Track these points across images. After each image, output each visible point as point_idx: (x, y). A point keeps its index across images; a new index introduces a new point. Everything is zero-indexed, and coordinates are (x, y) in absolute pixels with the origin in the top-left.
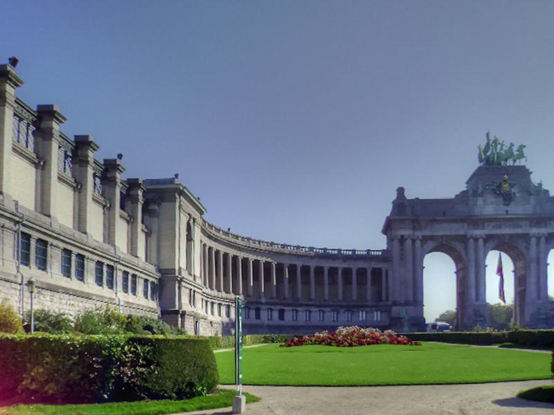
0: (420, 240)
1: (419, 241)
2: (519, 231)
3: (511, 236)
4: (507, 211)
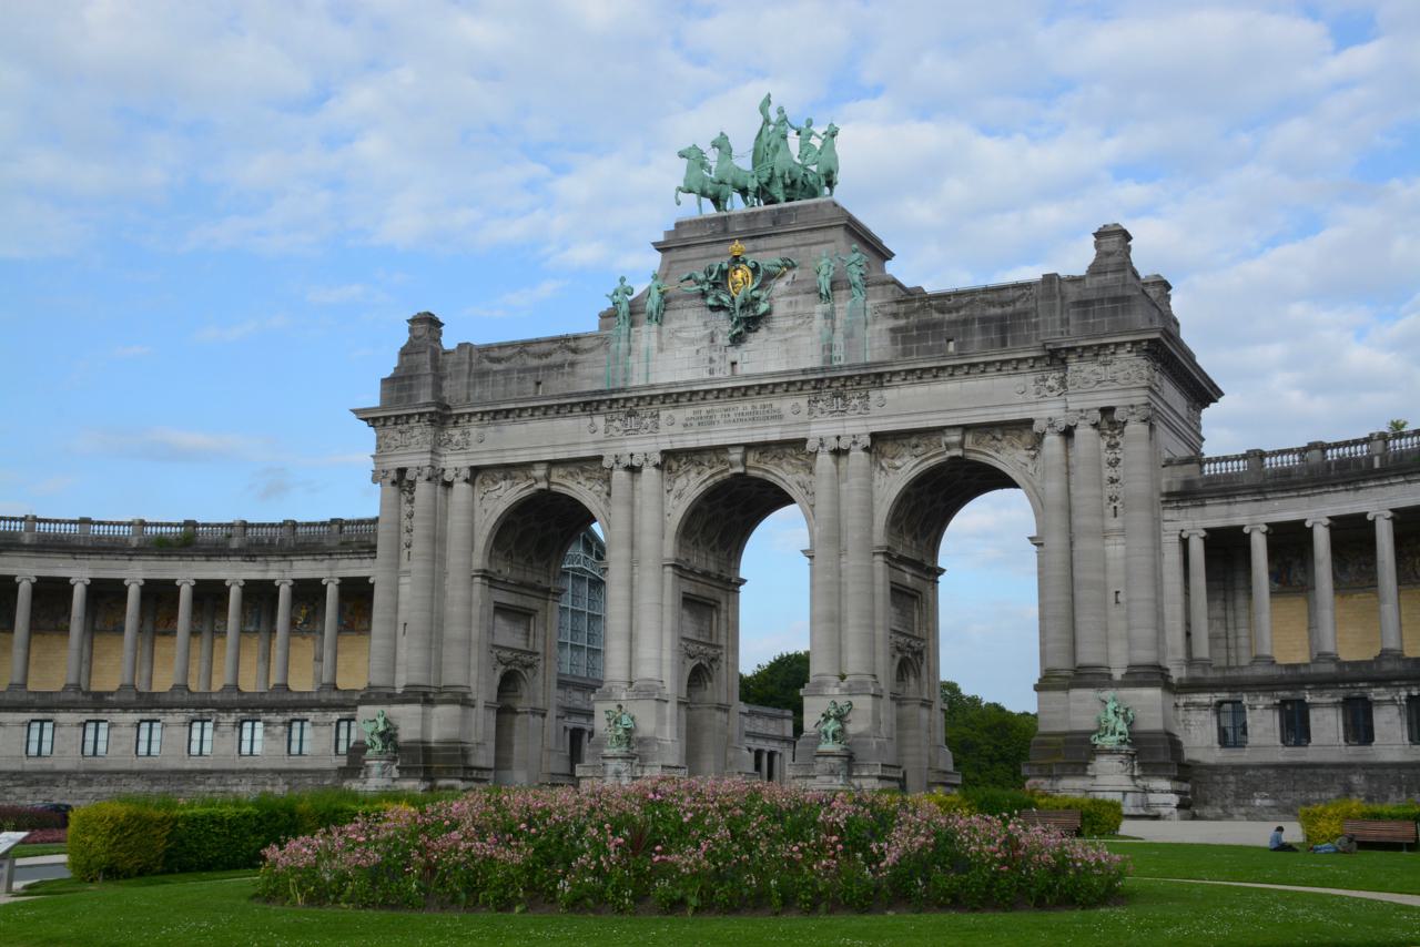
0: (466, 481)
1: (465, 485)
2: (773, 433)
3: (763, 447)
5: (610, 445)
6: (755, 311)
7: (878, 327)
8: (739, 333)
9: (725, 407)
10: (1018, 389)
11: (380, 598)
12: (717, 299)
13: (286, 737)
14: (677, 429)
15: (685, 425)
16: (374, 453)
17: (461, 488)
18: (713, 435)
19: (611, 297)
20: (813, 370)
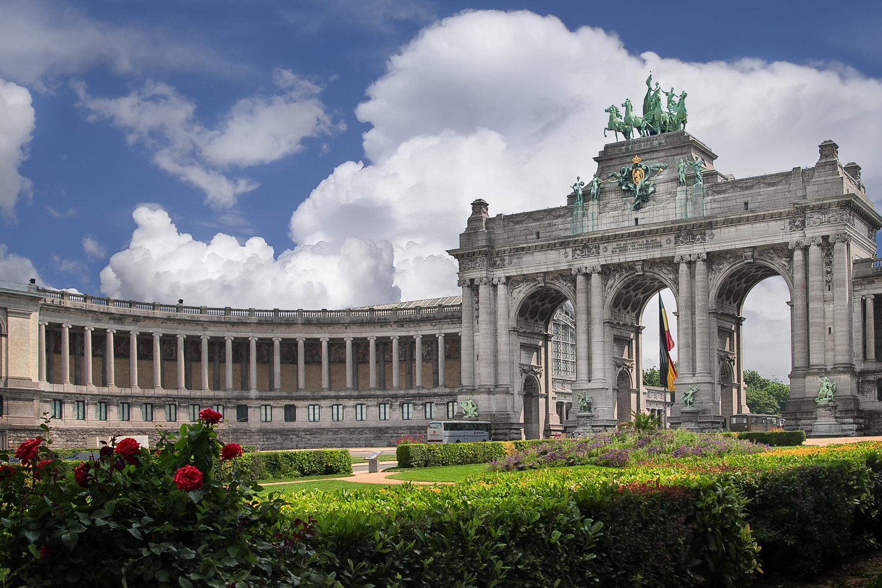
0: (504, 284)
1: (502, 286)
2: (657, 254)
3: (652, 263)
4: (636, 220)
5: (575, 263)
6: (646, 192)
7: (710, 198)
8: (639, 204)
9: (633, 241)
10: (781, 227)
11: (464, 344)
12: (627, 186)
13: (424, 411)
14: (609, 253)
16: (458, 272)
17: (502, 290)
19: (573, 188)
20: (676, 221)
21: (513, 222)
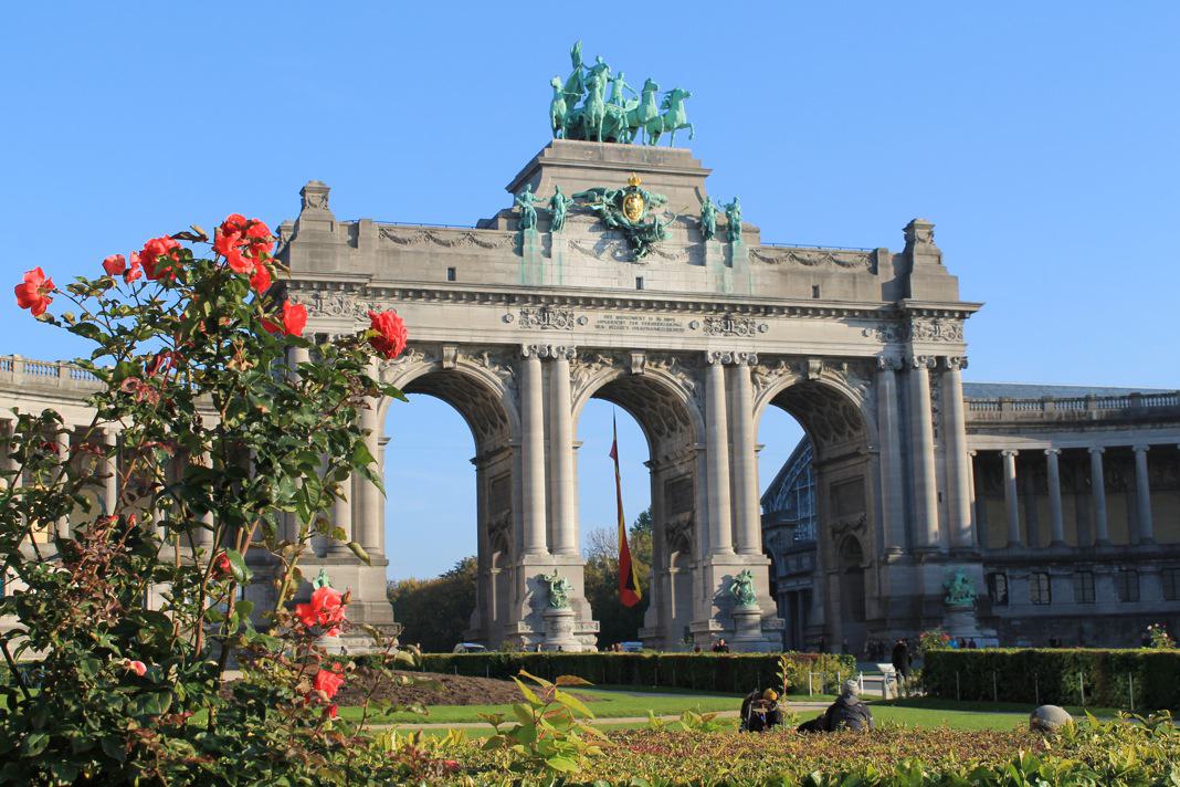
2: (677, 343)
3: (654, 355)
4: (639, 280)
5: (527, 335)
8: (645, 255)
12: (616, 219)
14: (589, 327)
15: (598, 327)
18: (624, 339)
21: (395, 240)
